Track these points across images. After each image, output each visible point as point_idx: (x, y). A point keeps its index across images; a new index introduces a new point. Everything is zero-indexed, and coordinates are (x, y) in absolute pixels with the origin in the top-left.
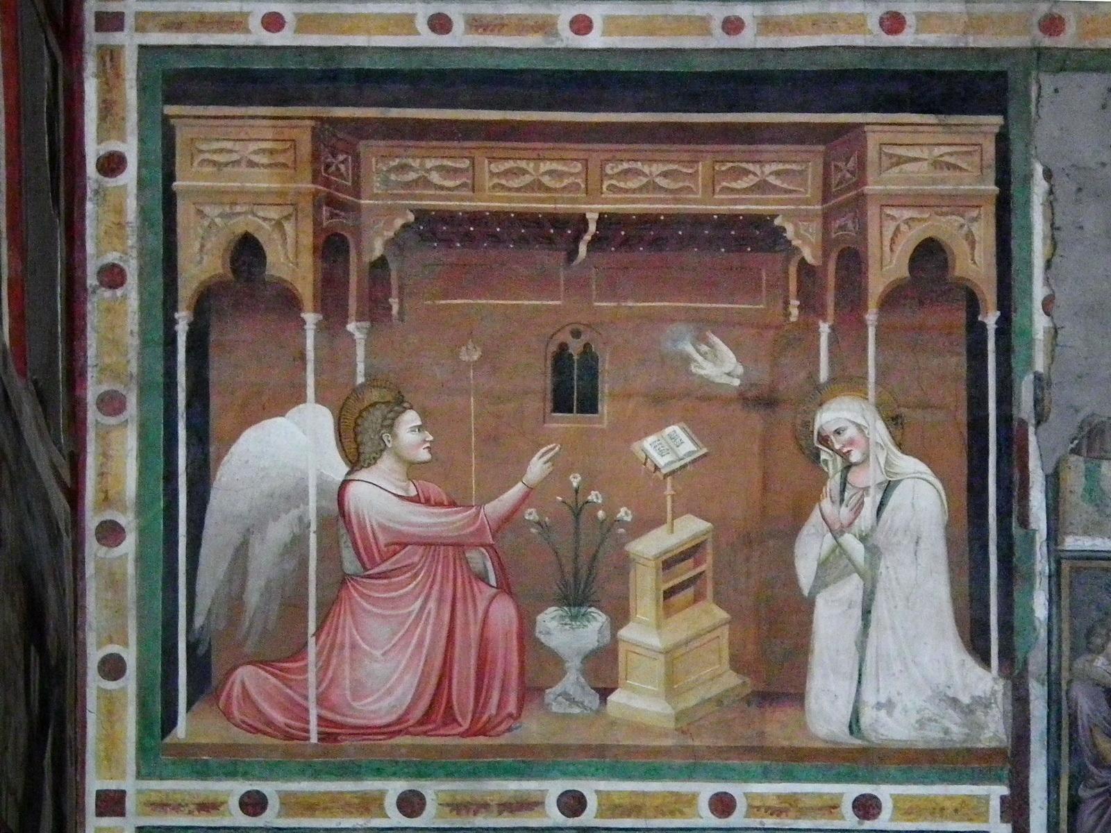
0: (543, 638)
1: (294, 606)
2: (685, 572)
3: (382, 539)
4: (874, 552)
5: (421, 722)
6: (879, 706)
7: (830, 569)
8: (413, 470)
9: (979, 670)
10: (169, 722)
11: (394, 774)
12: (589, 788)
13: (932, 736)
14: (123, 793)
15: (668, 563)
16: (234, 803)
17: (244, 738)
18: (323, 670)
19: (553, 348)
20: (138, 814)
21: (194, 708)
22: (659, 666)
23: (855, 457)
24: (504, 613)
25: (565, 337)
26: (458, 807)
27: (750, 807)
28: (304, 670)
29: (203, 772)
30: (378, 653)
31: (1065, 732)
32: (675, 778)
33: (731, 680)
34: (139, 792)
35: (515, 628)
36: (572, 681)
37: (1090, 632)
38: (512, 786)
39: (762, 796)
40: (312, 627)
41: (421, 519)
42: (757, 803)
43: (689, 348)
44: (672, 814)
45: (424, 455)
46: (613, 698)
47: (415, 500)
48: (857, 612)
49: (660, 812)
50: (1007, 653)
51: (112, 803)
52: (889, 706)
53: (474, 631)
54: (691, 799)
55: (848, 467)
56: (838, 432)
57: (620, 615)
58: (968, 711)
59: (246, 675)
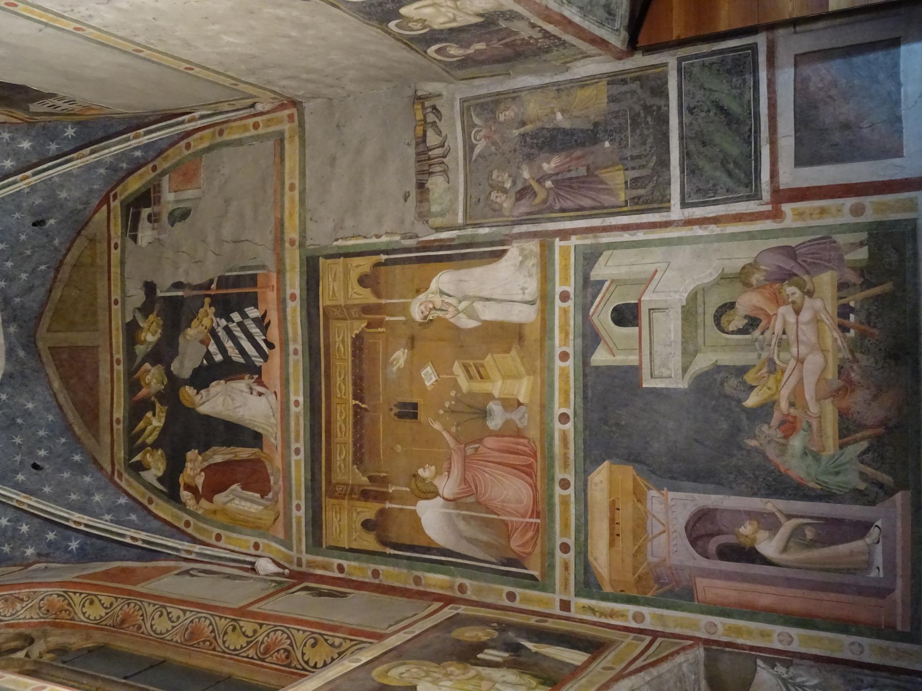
0: (499, 428)
1: (486, 523)
2: (473, 371)
3: (463, 486)
4: (465, 298)
5: (531, 477)
6: (524, 293)
7: (472, 315)
8: (438, 473)
9: (508, 254)
10: (532, 577)
11: (553, 490)
12: (558, 410)
13: (535, 271)
15: (471, 377)
16: (565, 556)
17: (538, 549)
18: (511, 514)
19: (396, 418)
21: (526, 566)
22: (509, 382)
23: (431, 306)
24: (490, 442)
25: (392, 413)
26: (566, 466)
28: (512, 521)
29: (552, 567)
30: (505, 492)
31: (534, 217)
32: (553, 376)
33: (514, 352)
35: (495, 438)
36: (515, 416)
37: (494, 210)
39: (560, 341)
40: (495, 517)
41: (456, 471)
43: (395, 368)
44: (568, 377)
45: (433, 468)
46: (521, 400)
47: (449, 472)
48: (487, 303)
49: (567, 382)
50: (502, 243)
51: (565, 605)
52: (523, 289)
53: (497, 454)
54: (562, 369)
55: (434, 308)
56: (422, 313)
57: (489, 397)
58: (525, 257)
59: (515, 543)
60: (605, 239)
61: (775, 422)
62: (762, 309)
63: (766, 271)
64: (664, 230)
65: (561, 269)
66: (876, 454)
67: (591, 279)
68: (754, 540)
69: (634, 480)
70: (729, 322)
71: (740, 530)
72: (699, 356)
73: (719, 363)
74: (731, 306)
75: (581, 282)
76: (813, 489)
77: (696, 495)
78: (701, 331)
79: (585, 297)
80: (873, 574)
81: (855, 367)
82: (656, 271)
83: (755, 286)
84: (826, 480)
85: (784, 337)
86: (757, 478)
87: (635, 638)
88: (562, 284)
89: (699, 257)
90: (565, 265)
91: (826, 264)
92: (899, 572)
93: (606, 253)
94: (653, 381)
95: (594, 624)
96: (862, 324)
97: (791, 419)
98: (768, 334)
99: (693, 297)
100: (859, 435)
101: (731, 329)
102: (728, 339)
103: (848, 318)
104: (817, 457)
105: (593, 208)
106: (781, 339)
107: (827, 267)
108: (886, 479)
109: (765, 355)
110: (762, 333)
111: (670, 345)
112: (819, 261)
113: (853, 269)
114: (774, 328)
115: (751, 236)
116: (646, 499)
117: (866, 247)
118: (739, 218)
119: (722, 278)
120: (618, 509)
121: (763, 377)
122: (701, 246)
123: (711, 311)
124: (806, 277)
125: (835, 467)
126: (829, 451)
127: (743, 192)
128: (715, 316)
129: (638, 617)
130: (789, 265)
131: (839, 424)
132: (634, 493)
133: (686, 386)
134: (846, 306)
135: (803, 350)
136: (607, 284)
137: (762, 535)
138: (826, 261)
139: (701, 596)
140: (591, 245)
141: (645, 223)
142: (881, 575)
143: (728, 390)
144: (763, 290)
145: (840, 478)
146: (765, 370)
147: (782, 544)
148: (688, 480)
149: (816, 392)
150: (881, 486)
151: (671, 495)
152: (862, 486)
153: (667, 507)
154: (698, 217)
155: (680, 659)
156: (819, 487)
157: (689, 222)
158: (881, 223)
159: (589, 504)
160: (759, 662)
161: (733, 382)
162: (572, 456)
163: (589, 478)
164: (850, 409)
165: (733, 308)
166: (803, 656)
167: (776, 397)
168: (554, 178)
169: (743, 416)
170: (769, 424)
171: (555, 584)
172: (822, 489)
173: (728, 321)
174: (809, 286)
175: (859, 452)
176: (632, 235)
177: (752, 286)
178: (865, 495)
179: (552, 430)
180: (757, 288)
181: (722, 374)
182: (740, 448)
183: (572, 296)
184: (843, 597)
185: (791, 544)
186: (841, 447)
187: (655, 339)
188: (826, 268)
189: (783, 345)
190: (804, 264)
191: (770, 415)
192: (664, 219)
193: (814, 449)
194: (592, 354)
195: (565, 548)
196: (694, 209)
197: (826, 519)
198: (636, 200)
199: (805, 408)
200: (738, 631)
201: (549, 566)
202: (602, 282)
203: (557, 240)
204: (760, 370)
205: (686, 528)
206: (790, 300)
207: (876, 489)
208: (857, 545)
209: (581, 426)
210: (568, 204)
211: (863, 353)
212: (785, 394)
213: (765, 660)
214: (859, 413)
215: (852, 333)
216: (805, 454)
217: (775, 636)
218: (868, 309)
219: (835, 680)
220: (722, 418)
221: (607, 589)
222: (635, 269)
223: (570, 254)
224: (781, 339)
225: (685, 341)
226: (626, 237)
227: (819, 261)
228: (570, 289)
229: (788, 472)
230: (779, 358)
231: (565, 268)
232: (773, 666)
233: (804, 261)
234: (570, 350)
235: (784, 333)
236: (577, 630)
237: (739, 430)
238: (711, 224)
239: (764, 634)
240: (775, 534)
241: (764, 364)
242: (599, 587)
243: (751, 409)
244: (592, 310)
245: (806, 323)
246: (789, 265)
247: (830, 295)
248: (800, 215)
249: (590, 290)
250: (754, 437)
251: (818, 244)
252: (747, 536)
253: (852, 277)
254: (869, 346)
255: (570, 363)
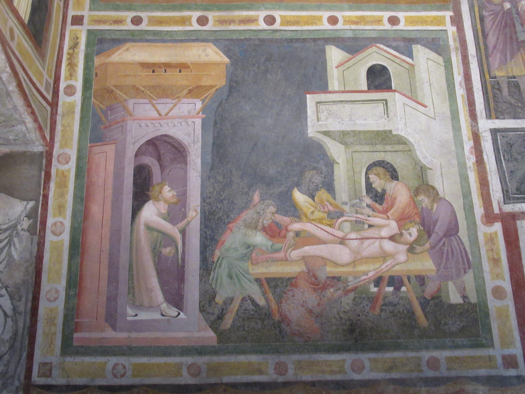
11: (196, 9)
14: (83, 17)
16: (129, 20)
20: (89, 25)
26: (222, 22)
27: (345, 21)
32: (312, 10)
34: (90, 16)
38: (245, 13)
42: (347, 19)
44: (312, 24)
49: (307, 23)
51: (78, 20)
54: (320, 19)
60: (456, 59)
61: (280, 218)
62: (392, 206)
63: (432, 209)
64: (468, 114)
65: (422, 17)
66: (252, 313)
67: (413, 46)
68: (157, 200)
69: (212, 87)
70: (378, 175)
71: (167, 186)
72: (342, 147)
73: (335, 166)
74: (394, 175)
75: (413, 35)
76: (213, 254)
77: (200, 144)
78: (367, 148)
79: (395, 40)
80: (130, 311)
81: (340, 292)
82: (425, 106)
83: (415, 199)
84: (223, 266)
85: (366, 226)
86: (221, 201)
87: (47, 83)
88: (406, 18)
89: (442, 146)
90: (426, 21)
91: (442, 265)
92: (134, 335)
93: (440, 59)
94: (314, 104)
95: (61, 48)
96: (384, 299)
97: (282, 233)
98: (368, 211)
99: (401, 141)
100: (270, 295)
101: (370, 176)
102: (360, 173)
103: (389, 285)
104: (246, 257)
105: (486, 46)
106: (364, 223)
107: (439, 265)
108: (228, 322)
109: (346, 208)
110: (368, 206)
111: (351, 120)
112: (445, 257)
113: (439, 290)
114: (375, 217)
115: (467, 195)
116: (192, 97)
117: (462, 302)
118: (484, 183)
119: (421, 167)
120: (180, 71)
121: (324, 208)
122: (453, 148)
123: (389, 158)
124: (427, 246)
125: (237, 276)
126: (253, 269)
127: (512, 187)
128: (383, 161)
129: (70, 90)
130: (440, 229)
131: (281, 278)
132: (197, 87)
133: (310, 135)
134: (402, 284)
135: (354, 244)
136: (409, 60)
137: (163, 207)
138: (446, 264)
139: (96, 149)
140: (448, 46)
141: (473, 95)
142: (129, 318)
143: (308, 174)
144: (412, 204)
145: (225, 279)
146: (331, 208)
147: (154, 225)
148: (214, 138)
149: (312, 257)
150: (221, 317)
151: (198, 122)
152: (219, 299)
153: (185, 118)
154: (482, 145)
155: (29, 120)
156: (215, 260)
157: (476, 137)
158: (487, 315)
159: (184, 44)
160: (31, 204)
161: (318, 179)
162: (232, 27)
163: (210, 44)
164: (297, 288)
165: (393, 178)
166: (41, 245)
167: (304, 219)
168: (514, 11)
169: (283, 189)
170: (277, 212)
171: (99, 11)
172: (214, 262)
173: (378, 173)
174: (419, 249)
175: (253, 296)
176: (460, 83)
177: (416, 196)
178: (210, 302)
179: (258, 9)
180: (414, 202)
181: (324, 169)
182: (250, 186)
183: (395, 28)
184: (104, 283)
185: (155, 234)
186: (258, 280)
187: (357, 106)
188: (438, 265)
189: (358, 225)
190: (441, 244)
191: (285, 213)
192: (478, 113)
193: (254, 255)
194: (337, 46)
195: (137, 21)
196: (490, 142)
197: (183, 266)
198: (497, 86)
199: (296, 247)
200: (62, 185)
201: (118, 5)
202: (411, 56)
203: (451, 14)
204: (331, 205)
205: (166, 136)
206: (403, 231)
207: (217, 312)
208: (159, 296)
209: (262, 36)
210: (488, 22)
211: (354, 300)
212: (309, 227)
213: (35, 209)
214: (293, 296)
215: (374, 290)
216: (249, 247)
217: (60, 219)
218: (399, 304)
219: (18, 276)
220: (279, 169)
221: (97, 61)
222: (426, 87)
223: (438, 25)
224: (364, 223)
225: (355, 133)
226: (458, 78)
227: (445, 257)
228: (402, 26)
229: (229, 230)
230: (344, 221)
231: (423, 21)
232: (29, 216)
233: (444, 244)
234: (340, 26)
235: (370, 226)
236: (53, 27)
237: (268, 185)
238: (477, 157)
239: (61, 208)
240: (165, 219)
241: (336, 207)
242: (99, 53)
243: (291, 195)
244: (382, 46)
245: (381, 248)
246: (440, 229)
247: (411, 268)
248: (491, 239)
249: (402, 44)
250: (262, 199)
251: (462, 256)
252: (160, 192)
253: (430, 289)
254: (362, 305)
255: (326, 26)
